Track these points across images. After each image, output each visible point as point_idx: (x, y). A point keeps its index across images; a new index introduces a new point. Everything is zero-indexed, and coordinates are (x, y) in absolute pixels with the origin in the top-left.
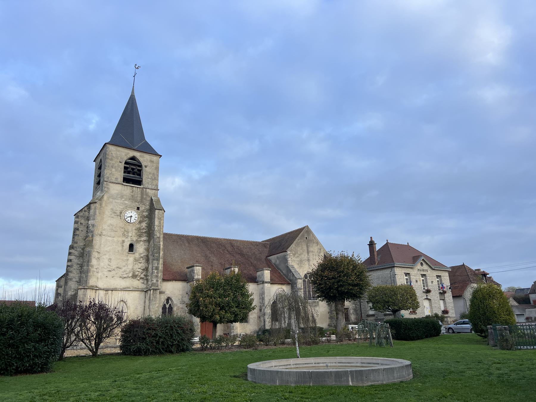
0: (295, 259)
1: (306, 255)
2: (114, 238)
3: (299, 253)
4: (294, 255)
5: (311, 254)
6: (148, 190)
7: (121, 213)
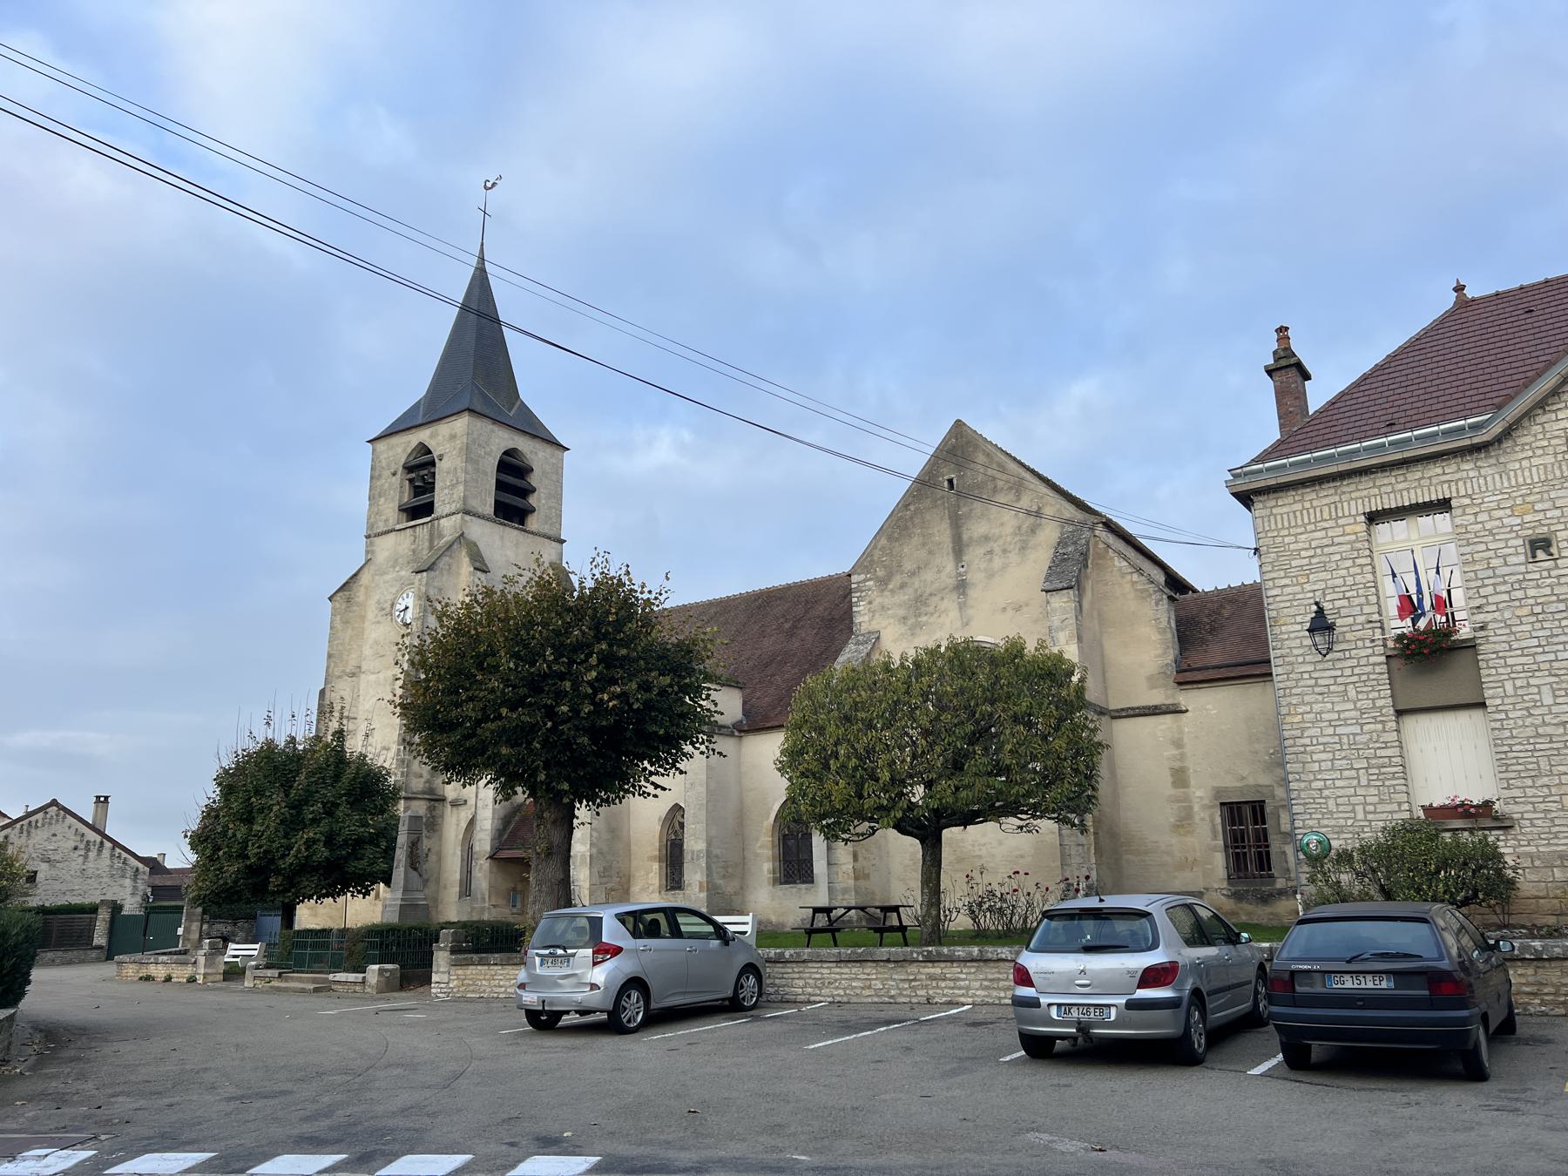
0: (887, 599)
1: (950, 566)
2: (381, 675)
3: (908, 566)
4: (883, 583)
5: (974, 555)
6: (442, 521)
7: (392, 605)
